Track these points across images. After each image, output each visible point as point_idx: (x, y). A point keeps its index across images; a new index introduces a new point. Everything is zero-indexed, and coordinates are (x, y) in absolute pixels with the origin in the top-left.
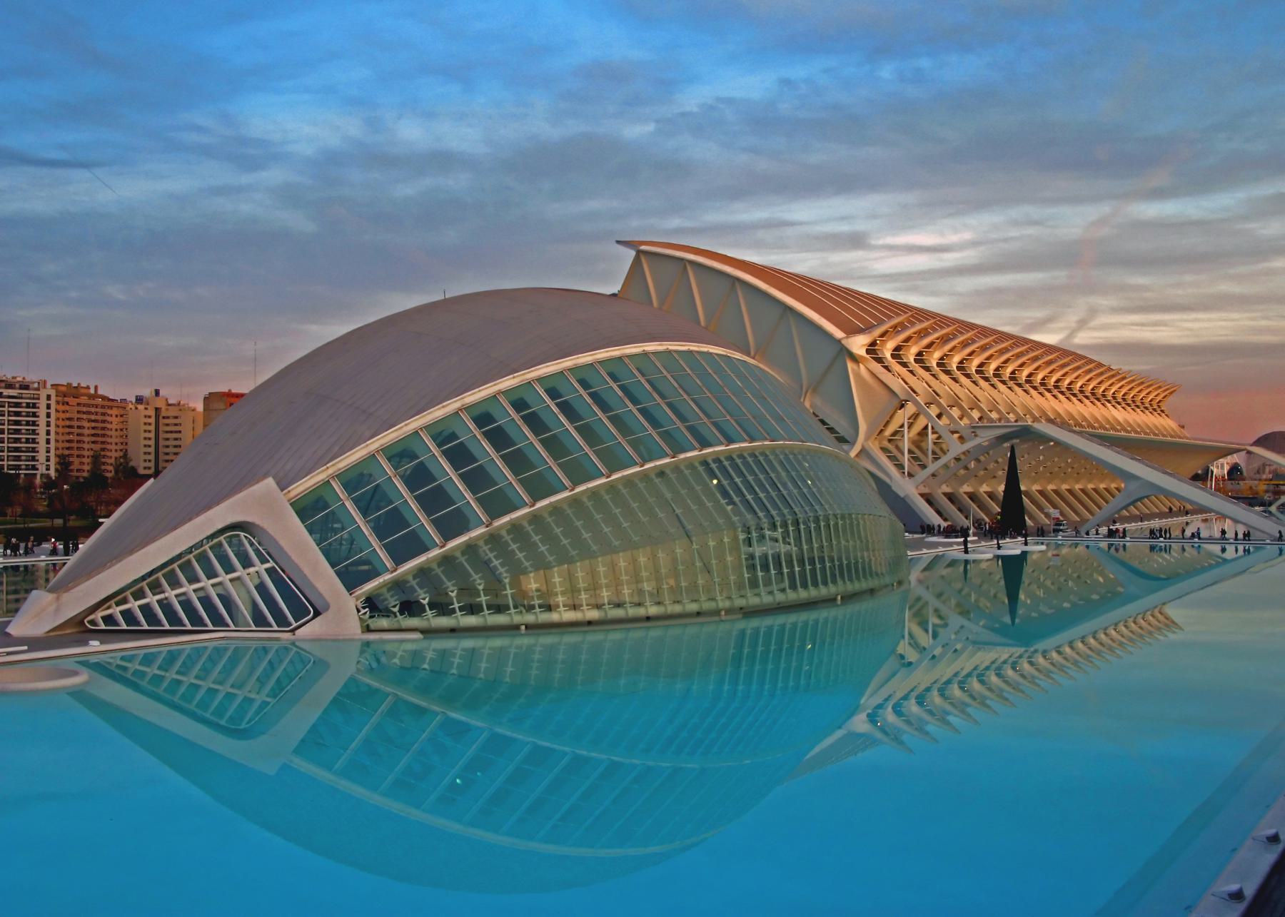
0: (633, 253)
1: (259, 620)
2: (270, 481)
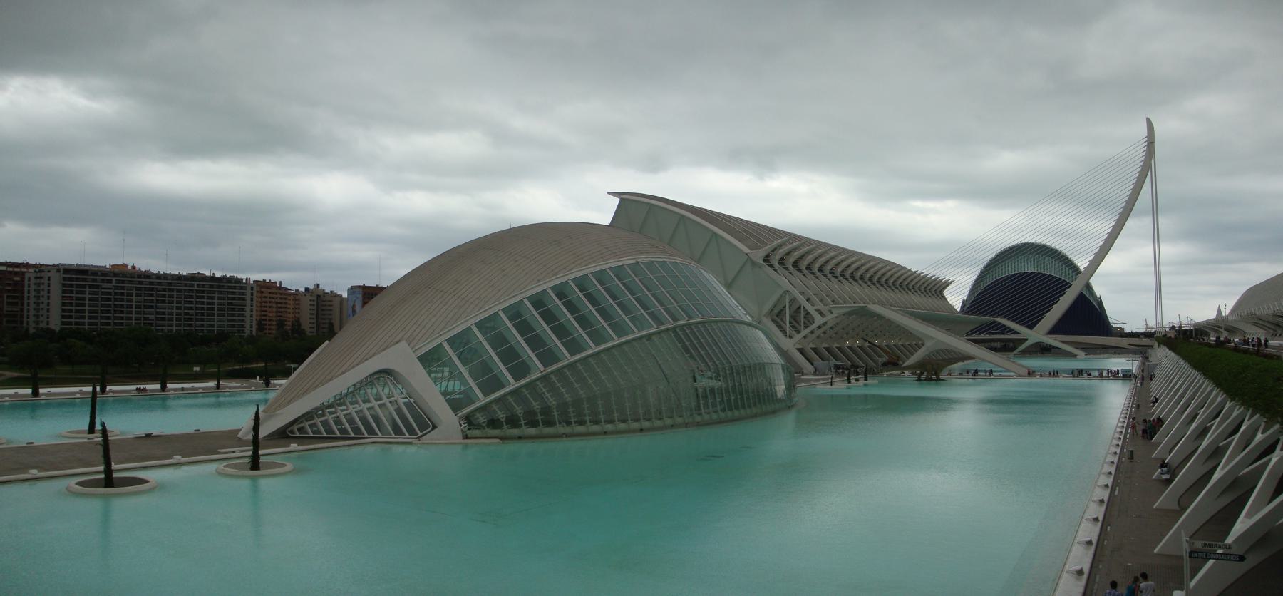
0: (616, 201)
1: (398, 431)
2: (403, 344)
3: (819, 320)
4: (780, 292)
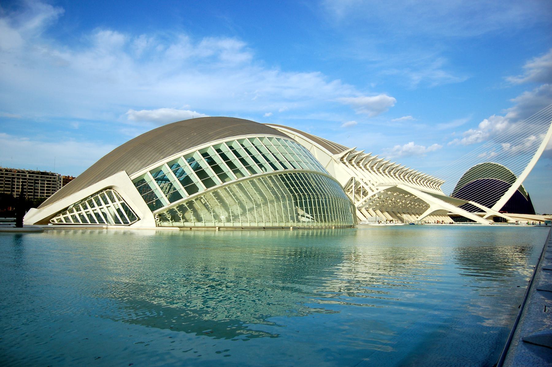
1: (117, 222)
2: (124, 173)
3: (370, 194)
4: (349, 178)
